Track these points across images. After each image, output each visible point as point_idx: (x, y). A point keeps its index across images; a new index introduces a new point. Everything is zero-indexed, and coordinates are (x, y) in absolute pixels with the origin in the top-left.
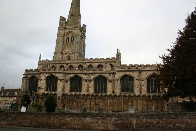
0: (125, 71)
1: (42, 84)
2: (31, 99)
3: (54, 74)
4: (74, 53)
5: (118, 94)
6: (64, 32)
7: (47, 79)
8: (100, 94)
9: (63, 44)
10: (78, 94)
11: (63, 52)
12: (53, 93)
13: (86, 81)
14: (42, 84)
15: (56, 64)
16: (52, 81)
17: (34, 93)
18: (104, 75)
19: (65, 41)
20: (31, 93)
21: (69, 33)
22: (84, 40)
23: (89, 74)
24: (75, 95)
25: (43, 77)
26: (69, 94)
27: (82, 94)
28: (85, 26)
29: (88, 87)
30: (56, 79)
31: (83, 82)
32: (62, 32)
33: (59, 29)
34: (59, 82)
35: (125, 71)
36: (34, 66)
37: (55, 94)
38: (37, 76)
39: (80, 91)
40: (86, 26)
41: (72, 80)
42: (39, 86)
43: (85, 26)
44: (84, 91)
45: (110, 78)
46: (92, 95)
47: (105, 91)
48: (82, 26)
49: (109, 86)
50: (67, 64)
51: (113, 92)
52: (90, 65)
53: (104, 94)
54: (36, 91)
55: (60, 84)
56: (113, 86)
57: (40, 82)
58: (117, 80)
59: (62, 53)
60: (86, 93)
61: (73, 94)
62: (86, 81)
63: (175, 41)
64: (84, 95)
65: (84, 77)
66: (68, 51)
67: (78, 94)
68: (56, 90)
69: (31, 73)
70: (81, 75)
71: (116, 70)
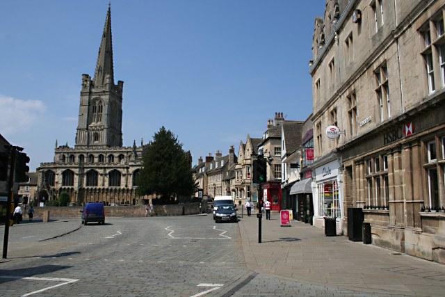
0: (138, 166)
1: (59, 178)
2: (49, 194)
3: (71, 169)
4: (102, 130)
5: (130, 188)
6: (90, 98)
7: (64, 173)
8: (114, 188)
9: (88, 115)
10: (94, 188)
11: (89, 128)
12: (70, 187)
13: (101, 175)
14: (59, 178)
15: (75, 153)
16: (68, 175)
17: (52, 187)
18: (119, 169)
19: (91, 111)
20: (49, 188)
21: (96, 99)
22: (121, 106)
23: (105, 168)
24: (92, 189)
25: (59, 171)
26: (86, 188)
27: (98, 187)
28: (121, 83)
29: (104, 181)
30: (73, 173)
31: (99, 176)
32: (86, 98)
33: (82, 94)
34: (75, 176)
35: (138, 166)
36: (50, 157)
37: (72, 189)
38: (54, 170)
39: (97, 185)
40: (123, 82)
41: (88, 174)
42: (56, 180)
43: (121, 83)
44: (100, 186)
45: (124, 173)
46: (107, 189)
47: (119, 185)
48: (116, 83)
49: (123, 179)
50: (88, 153)
51: (126, 186)
52: (111, 155)
53: (118, 188)
54: (53, 185)
55: (76, 178)
56: (127, 180)
57: (56, 176)
58: (130, 175)
59: (87, 129)
60: (102, 187)
61: (90, 187)
62: (101, 175)
63: (179, 141)
64: (100, 189)
65: (101, 171)
66: (96, 127)
67: (94, 188)
68: (73, 185)
69: (47, 166)
70: (97, 170)
71: (130, 164)
